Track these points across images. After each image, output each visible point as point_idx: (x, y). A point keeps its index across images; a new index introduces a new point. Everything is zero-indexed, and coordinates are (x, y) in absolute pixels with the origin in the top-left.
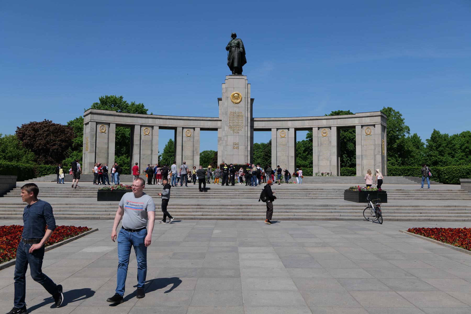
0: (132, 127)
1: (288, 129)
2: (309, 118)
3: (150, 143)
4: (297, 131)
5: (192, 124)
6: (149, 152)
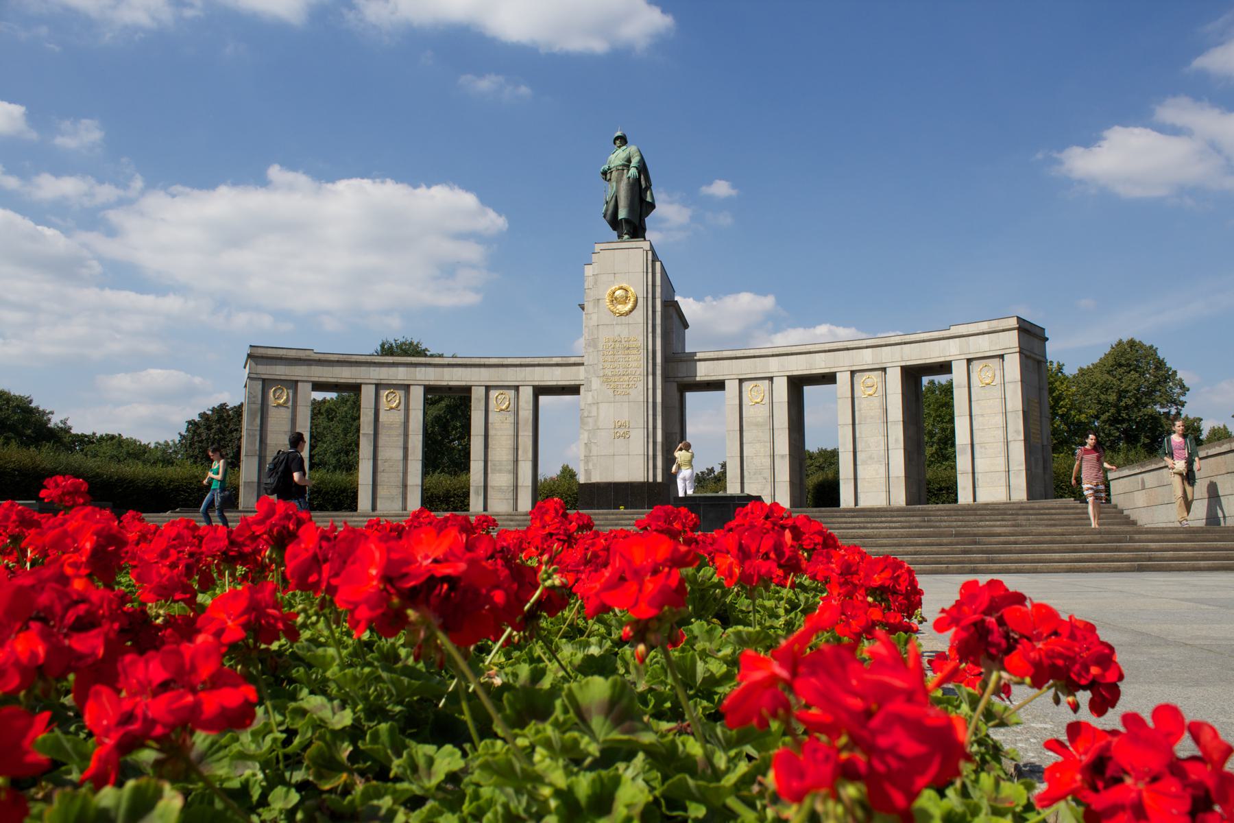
0: (356, 388)
1: (771, 379)
2: (827, 347)
3: (401, 431)
4: (805, 388)
5: (511, 376)
6: (399, 454)
